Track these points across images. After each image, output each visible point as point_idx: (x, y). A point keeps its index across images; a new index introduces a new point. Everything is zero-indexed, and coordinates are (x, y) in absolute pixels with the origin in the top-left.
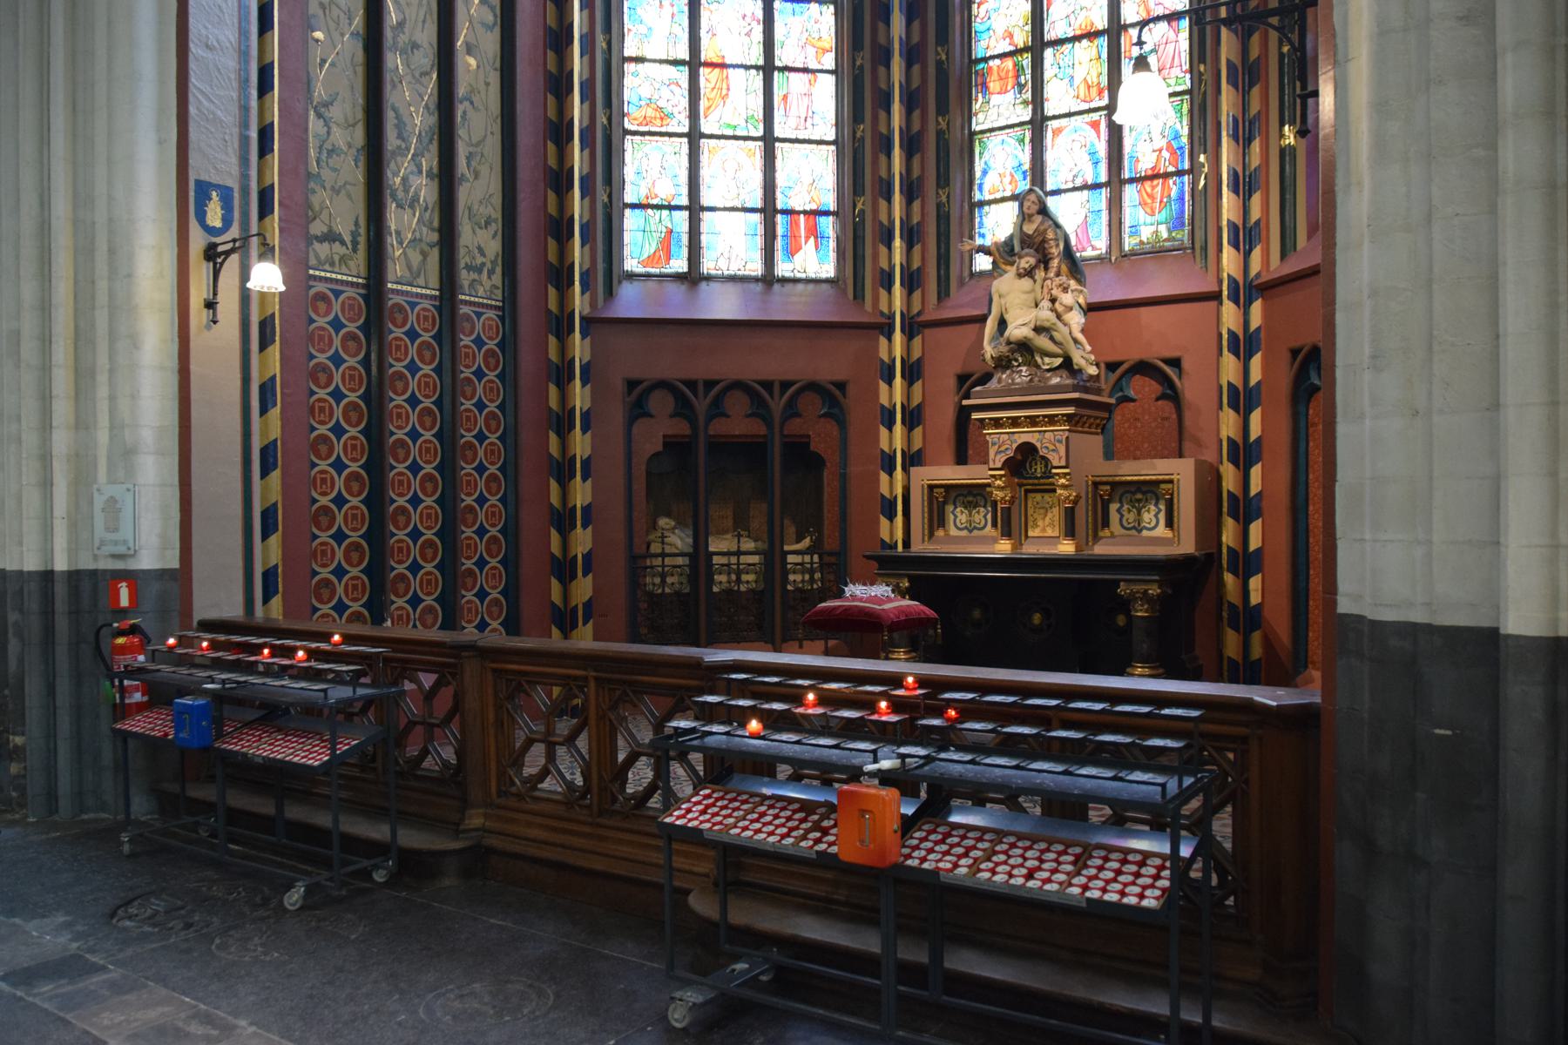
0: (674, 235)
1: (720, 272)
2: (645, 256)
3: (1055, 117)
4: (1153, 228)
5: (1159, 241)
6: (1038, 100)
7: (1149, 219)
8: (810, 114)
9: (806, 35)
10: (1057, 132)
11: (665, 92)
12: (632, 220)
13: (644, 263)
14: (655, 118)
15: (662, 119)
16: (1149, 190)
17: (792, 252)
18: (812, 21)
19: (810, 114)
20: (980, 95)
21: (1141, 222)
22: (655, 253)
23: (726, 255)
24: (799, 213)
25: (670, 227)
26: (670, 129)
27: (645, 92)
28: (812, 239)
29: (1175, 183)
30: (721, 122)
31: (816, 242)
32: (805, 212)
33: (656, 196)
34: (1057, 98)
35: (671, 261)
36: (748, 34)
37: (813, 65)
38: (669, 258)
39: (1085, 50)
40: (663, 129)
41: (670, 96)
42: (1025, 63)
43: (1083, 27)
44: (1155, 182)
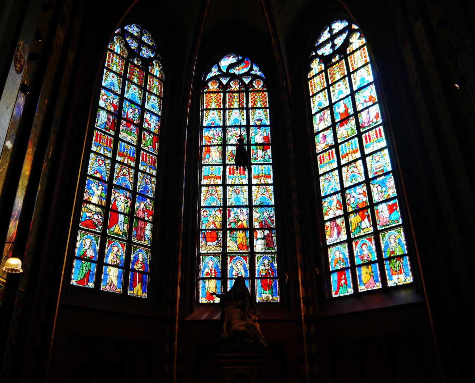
0: (91, 273)
1: (107, 291)
2: (79, 279)
3: (231, 253)
4: (267, 295)
5: (269, 300)
6: (224, 246)
7: (265, 292)
8: (144, 235)
9: (145, 208)
10: (231, 258)
11: (96, 217)
12: (76, 263)
13: (78, 282)
14: (91, 225)
15: (93, 226)
16: (265, 282)
17: (133, 286)
18: (147, 204)
19: (144, 235)
20: (203, 241)
21: (263, 292)
22: (83, 279)
23: (110, 284)
24: (137, 271)
25: (90, 268)
26: (95, 230)
27: (89, 215)
28: (140, 283)
29: (273, 281)
30: (114, 232)
31: (142, 284)
32: (139, 271)
33: (87, 255)
34: (232, 247)
35: (89, 284)
36: (127, 203)
37: (146, 219)
38: (87, 282)
39: (240, 234)
40: (93, 230)
41: (97, 218)
42: (220, 234)
43: (240, 226)
44: (267, 280)
